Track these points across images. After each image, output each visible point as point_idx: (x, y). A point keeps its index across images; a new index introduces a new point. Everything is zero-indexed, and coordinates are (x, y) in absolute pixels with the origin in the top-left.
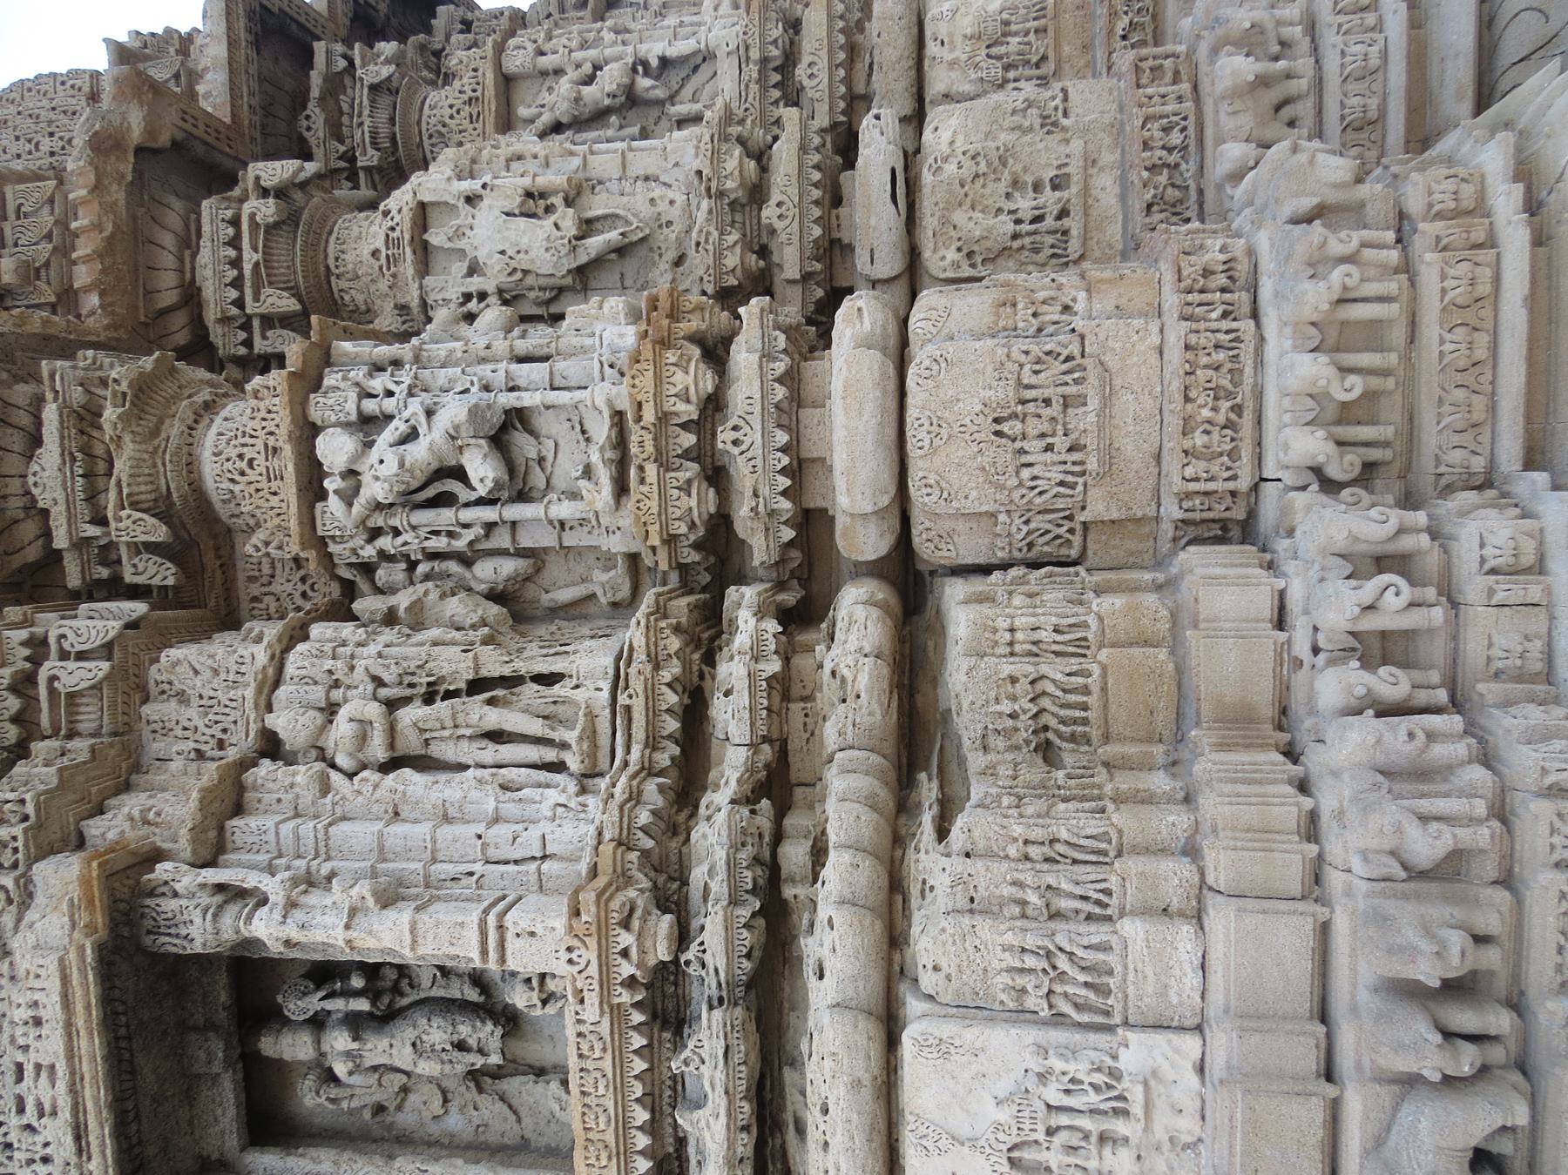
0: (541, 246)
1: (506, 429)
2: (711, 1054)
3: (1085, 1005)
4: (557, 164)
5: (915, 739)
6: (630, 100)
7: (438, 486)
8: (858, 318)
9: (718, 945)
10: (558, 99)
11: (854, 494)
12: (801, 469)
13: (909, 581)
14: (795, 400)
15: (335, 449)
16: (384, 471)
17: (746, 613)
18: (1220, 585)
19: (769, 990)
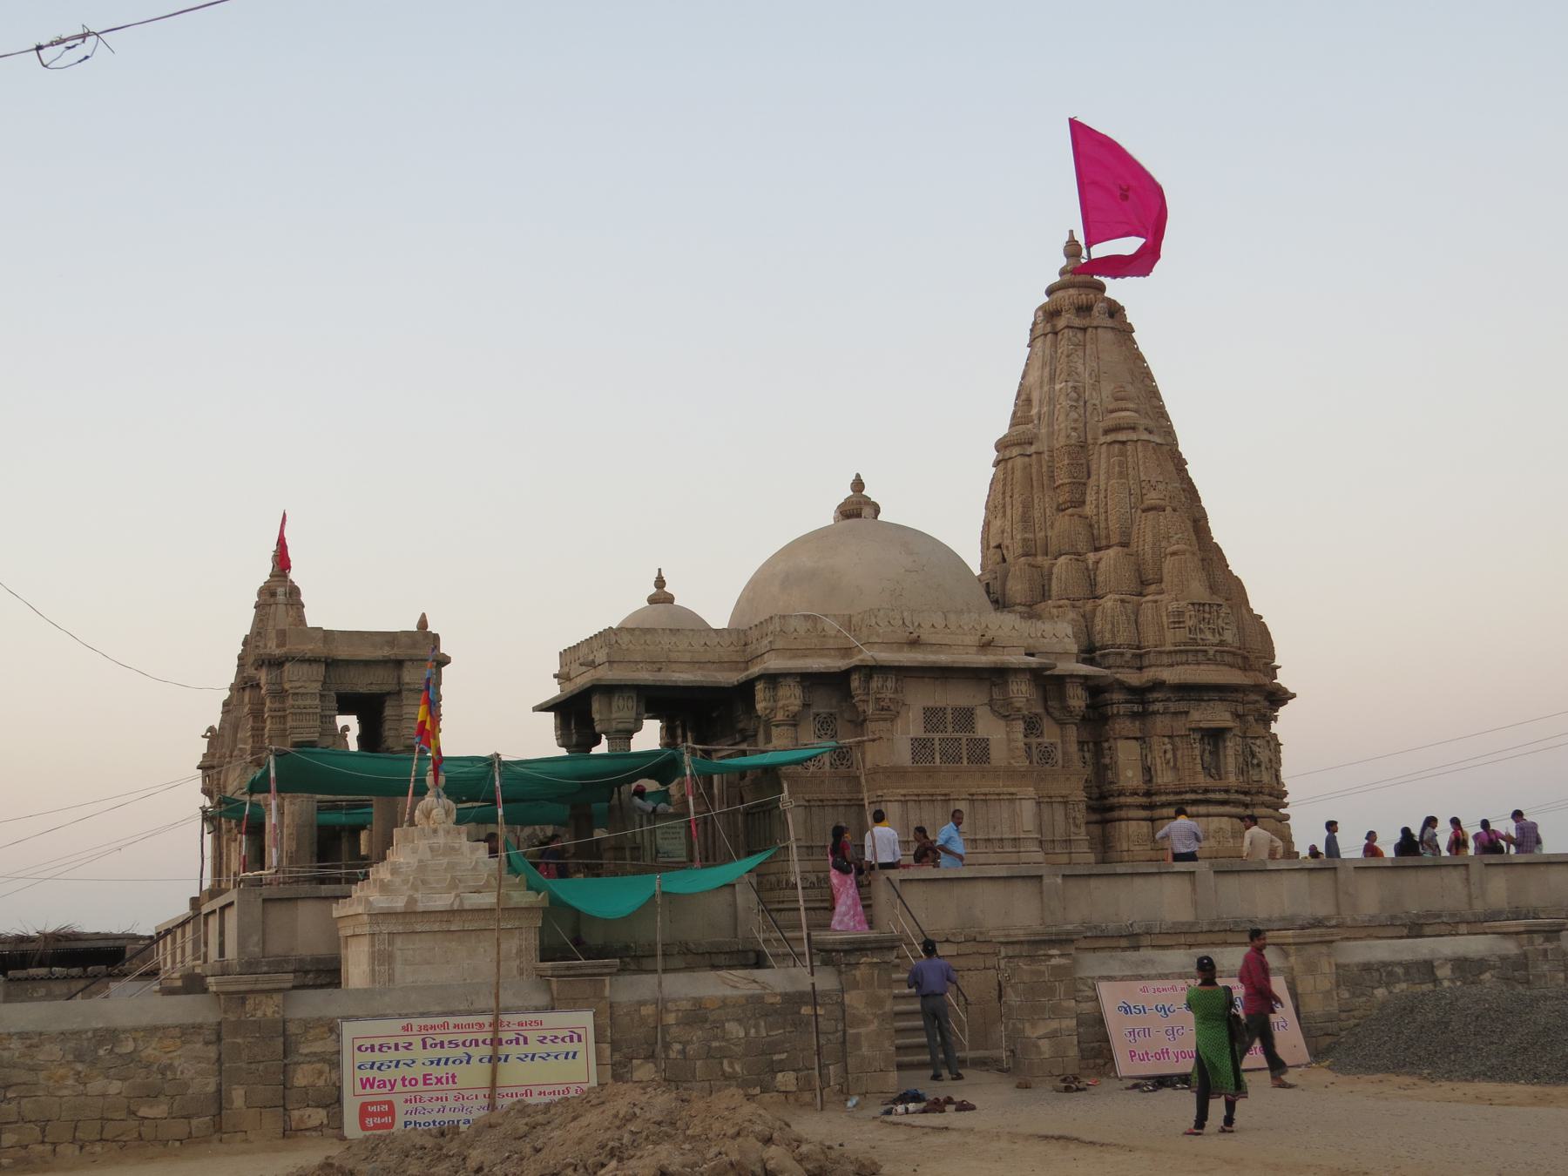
2: (1223, 796)
7: (1253, 755)
9: (1234, 797)
12: (1254, 805)
15: (1258, 742)
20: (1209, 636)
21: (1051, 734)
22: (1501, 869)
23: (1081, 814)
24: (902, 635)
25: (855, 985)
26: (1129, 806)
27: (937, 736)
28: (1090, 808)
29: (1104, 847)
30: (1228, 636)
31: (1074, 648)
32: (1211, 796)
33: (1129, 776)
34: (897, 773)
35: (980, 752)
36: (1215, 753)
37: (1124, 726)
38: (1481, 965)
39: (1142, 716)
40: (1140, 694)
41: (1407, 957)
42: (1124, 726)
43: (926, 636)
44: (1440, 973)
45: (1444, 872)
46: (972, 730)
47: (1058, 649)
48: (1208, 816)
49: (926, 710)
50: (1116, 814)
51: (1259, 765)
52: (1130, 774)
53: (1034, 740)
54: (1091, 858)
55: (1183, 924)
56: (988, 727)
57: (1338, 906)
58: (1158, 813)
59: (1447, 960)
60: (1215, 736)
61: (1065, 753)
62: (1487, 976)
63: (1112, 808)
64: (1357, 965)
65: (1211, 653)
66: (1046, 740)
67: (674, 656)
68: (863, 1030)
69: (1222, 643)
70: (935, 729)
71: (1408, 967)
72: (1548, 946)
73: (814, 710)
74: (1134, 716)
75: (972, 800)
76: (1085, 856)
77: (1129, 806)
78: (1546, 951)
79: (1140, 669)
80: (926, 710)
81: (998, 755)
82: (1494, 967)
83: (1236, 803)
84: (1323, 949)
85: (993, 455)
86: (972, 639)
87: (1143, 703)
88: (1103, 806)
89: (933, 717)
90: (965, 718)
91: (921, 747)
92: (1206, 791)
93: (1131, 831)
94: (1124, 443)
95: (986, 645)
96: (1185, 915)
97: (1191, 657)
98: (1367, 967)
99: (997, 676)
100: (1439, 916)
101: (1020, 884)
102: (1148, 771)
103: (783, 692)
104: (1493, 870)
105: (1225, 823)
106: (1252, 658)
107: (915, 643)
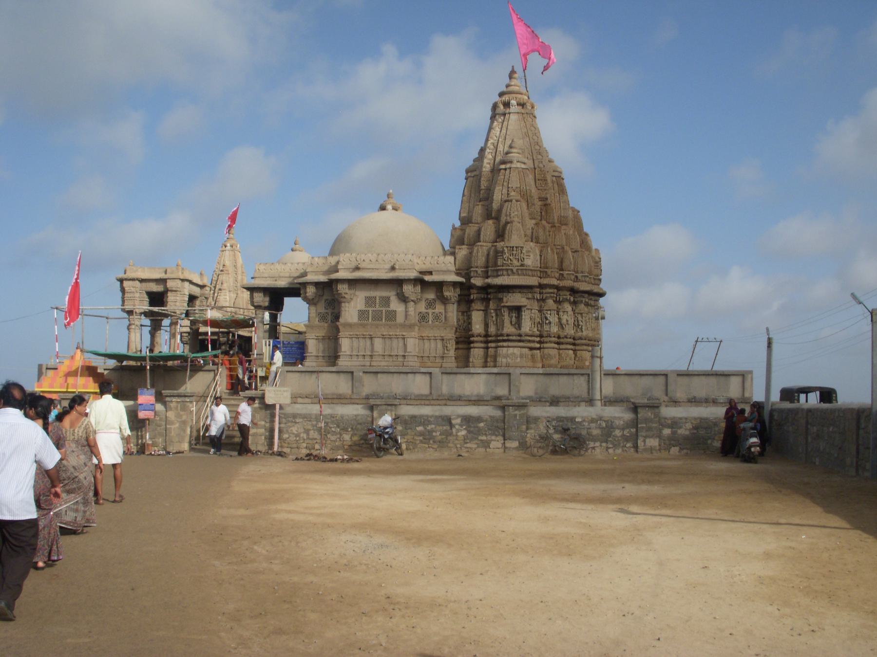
0: (564, 321)
1: (550, 323)
2: (519, 338)
3: (521, 356)
4: (571, 321)
5: (531, 349)
6: (579, 325)
7: (546, 319)
8: (556, 346)
9: (523, 338)
10: (580, 318)
11: (545, 345)
13: (539, 349)
14: (551, 342)
16: (548, 316)
17: (538, 339)
18: (540, 365)
19: (520, 341)
20: (515, 262)
21: (439, 308)
22: (611, 377)
23: (452, 346)
24: (353, 265)
25: (171, 409)
26: (477, 342)
27: (370, 309)
28: (457, 343)
29: (464, 361)
30: (529, 262)
31: (453, 268)
32: (511, 338)
33: (477, 327)
34: (350, 325)
35: (392, 315)
36: (519, 317)
37: (478, 305)
38: (479, 419)
39: (486, 300)
40: (486, 289)
41: (437, 414)
42: (478, 305)
43: (362, 265)
44: (453, 422)
45: (575, 377)
46: (389, 306)
47: (445, 269)
48: (509, 347)
49: (366, 298)
50: (472, 345)
51: (550, 323)
52: (478, 327)
53: (430, 311)
54: (455, 365)
55: (422, 395)
56: (396, 305)
57: (510, 391)
58: (490, 345)
59: (458, 416)
60: (518, 309)
61: (445, 317)
62: (482, 425)
63: (473, 342)
64: (409, 416)
65: (515, 270)
66: (437, 311)
67: (282, 275)
68: (173, 427)
69: (522, 265)
70: (370, 306)
71: (437, 417)
72: (517, 412)
73: (325, 297)
74: (483, 300)
75: (383, 337)
76: (451, 364)
77: (477, 342)
78: (516, 415)
79: (487, 277)
80: (366, 298)
81: (400, 319)
82: (486, 421)
83: (529, 341)
84: (389, 408)
85: (464, 175)
86: (388, 266)
87: (488, 294)
88: (465, 340)
89: (370, 301)
90: (386, 301)
91: (362, 314)
92: (508, 335)
93: (477, 353)
94: (505, 169)
95: (393, 268)
96: (426, 391)
97: (505, 273)
98: (413, 417)
99: (398, 283)
100: (569, 398)
101: (342, 375)
102: (486, 326)
103: (308, 290)
104: (368, 375)
105: (517, 351)
106: (549, 271)
107: (357, 268)
